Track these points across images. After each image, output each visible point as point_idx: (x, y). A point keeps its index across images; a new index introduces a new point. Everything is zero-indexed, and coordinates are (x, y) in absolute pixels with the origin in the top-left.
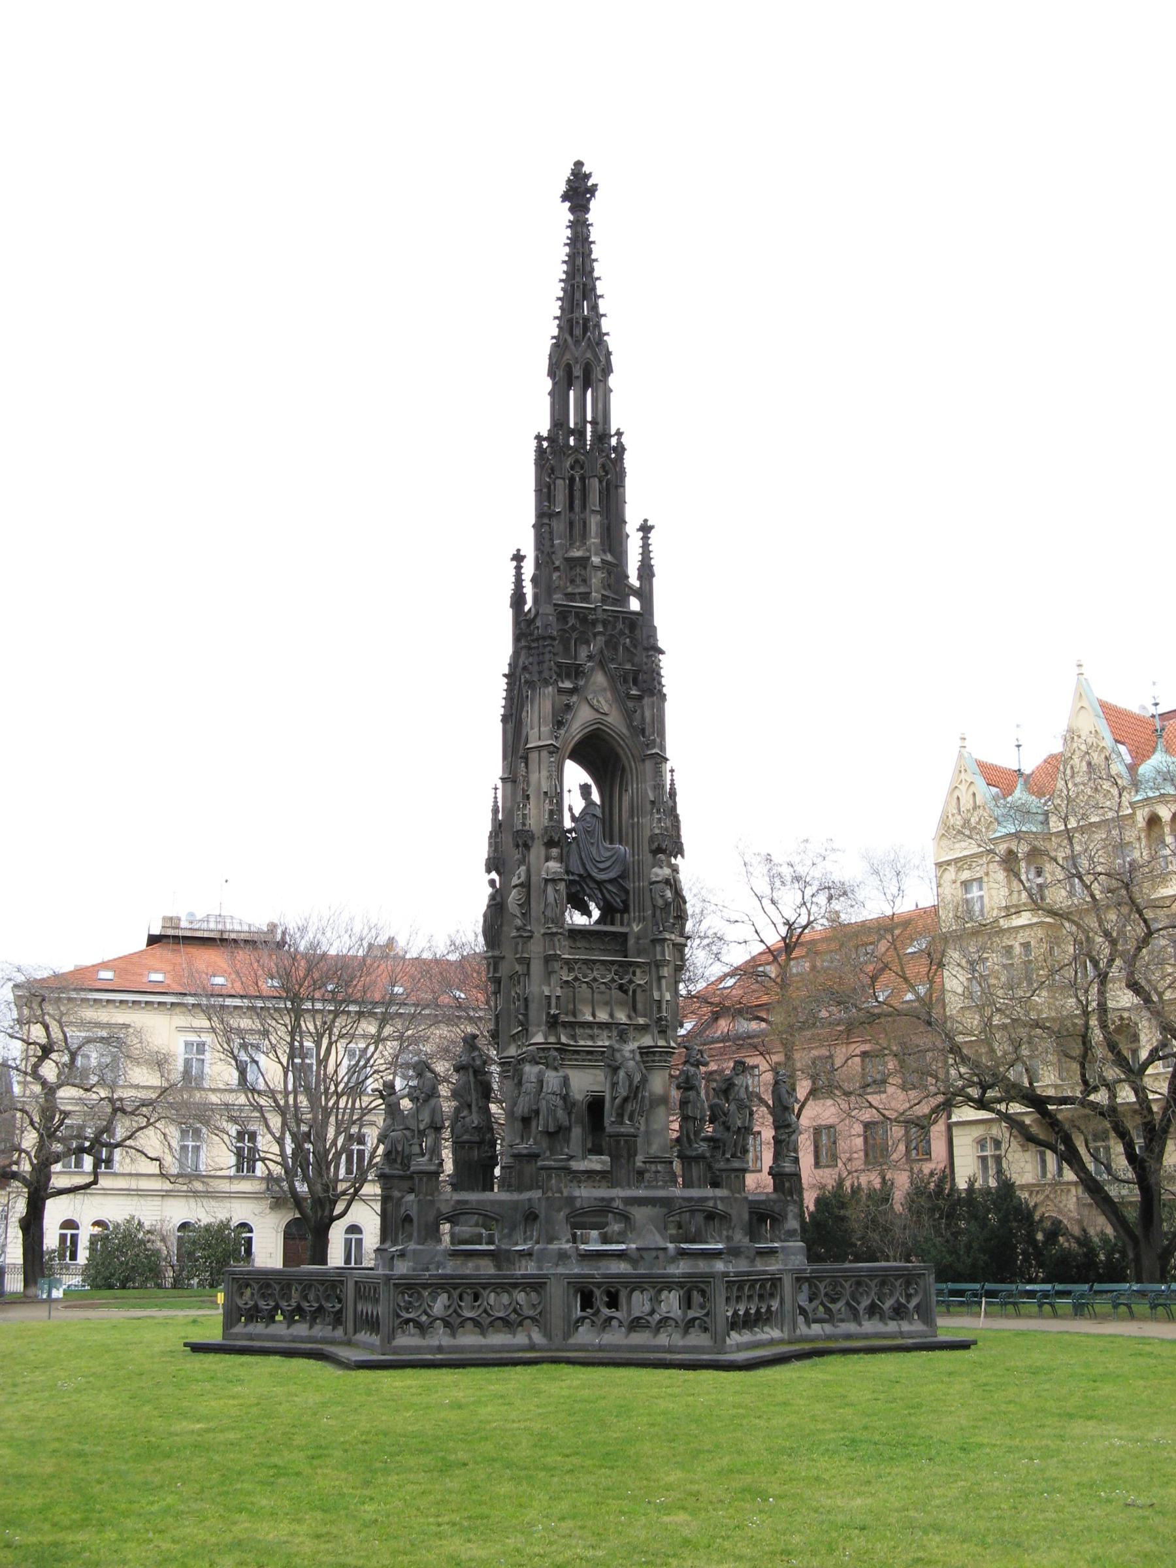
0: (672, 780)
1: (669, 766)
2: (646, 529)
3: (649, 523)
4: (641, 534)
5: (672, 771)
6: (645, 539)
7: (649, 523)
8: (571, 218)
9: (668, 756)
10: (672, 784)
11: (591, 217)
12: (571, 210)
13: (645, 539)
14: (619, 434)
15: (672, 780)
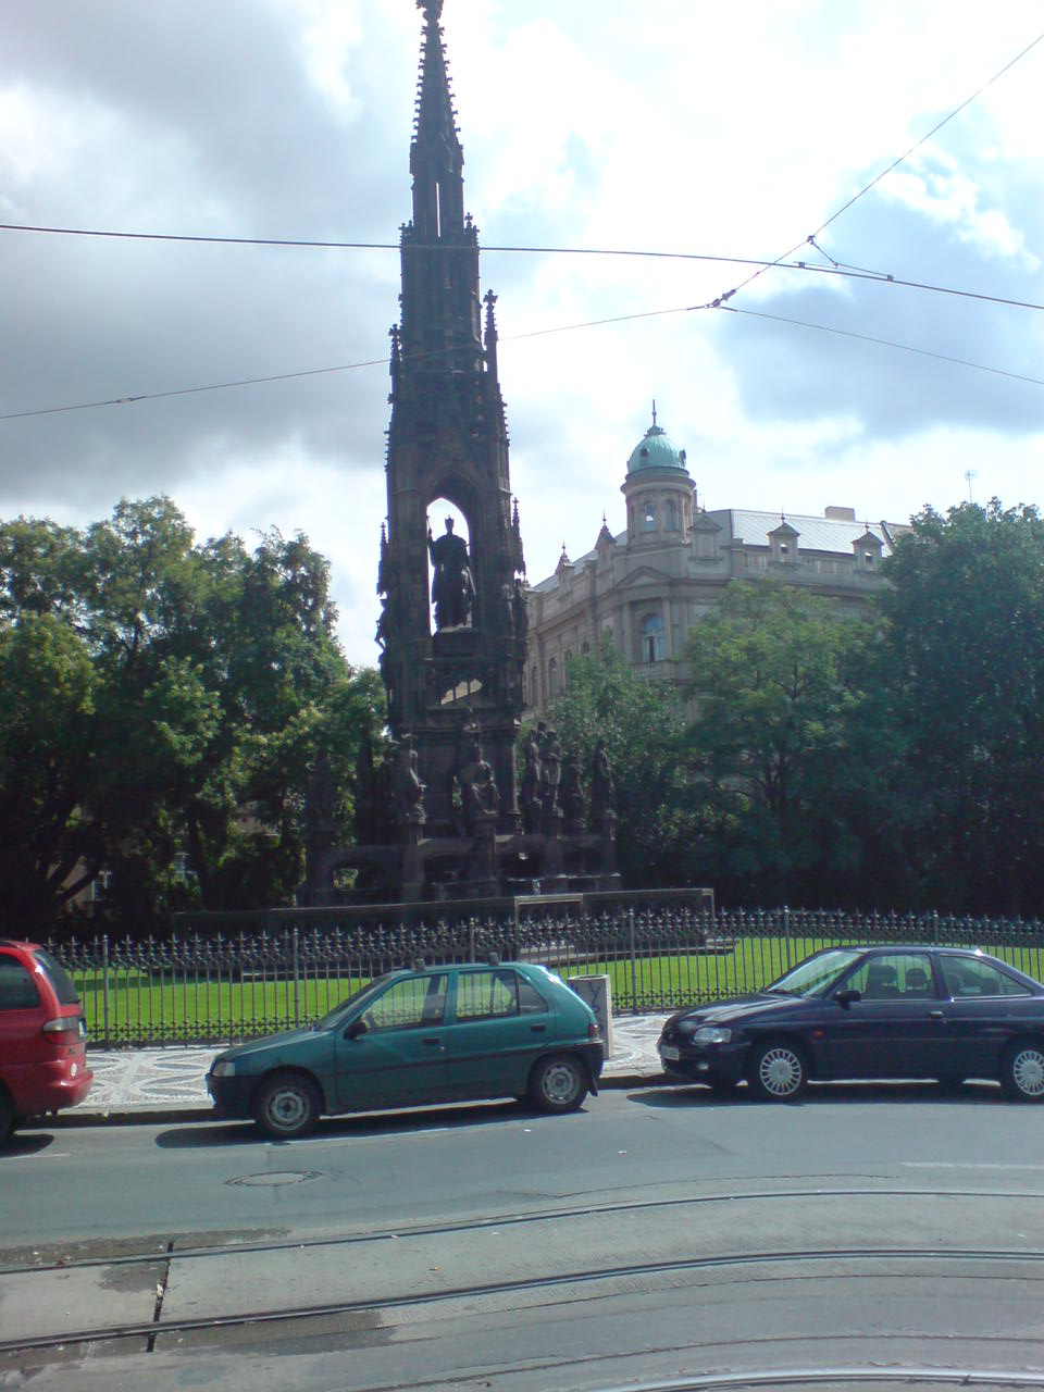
0: (516, 510)
1: (512, 499)
2: (491, 298)
3: (494, 294)
4: (486, 304)
5: (516, 502)
6: (490, 308)
7: (494, 294)
8: (425, 23)
9: (512, 490)
10: (516, 513)
11: (441, 22)
12: (426, 16)
13: (490, 308)
14: (469, 218)
15: (516, 510)
